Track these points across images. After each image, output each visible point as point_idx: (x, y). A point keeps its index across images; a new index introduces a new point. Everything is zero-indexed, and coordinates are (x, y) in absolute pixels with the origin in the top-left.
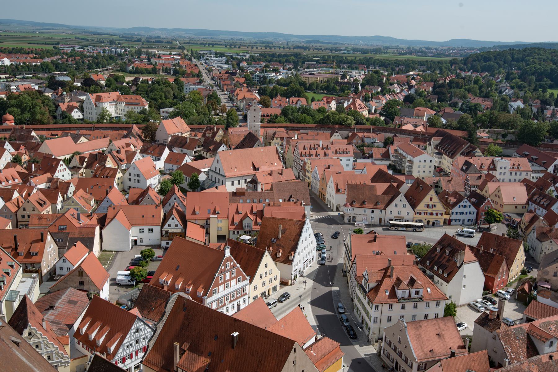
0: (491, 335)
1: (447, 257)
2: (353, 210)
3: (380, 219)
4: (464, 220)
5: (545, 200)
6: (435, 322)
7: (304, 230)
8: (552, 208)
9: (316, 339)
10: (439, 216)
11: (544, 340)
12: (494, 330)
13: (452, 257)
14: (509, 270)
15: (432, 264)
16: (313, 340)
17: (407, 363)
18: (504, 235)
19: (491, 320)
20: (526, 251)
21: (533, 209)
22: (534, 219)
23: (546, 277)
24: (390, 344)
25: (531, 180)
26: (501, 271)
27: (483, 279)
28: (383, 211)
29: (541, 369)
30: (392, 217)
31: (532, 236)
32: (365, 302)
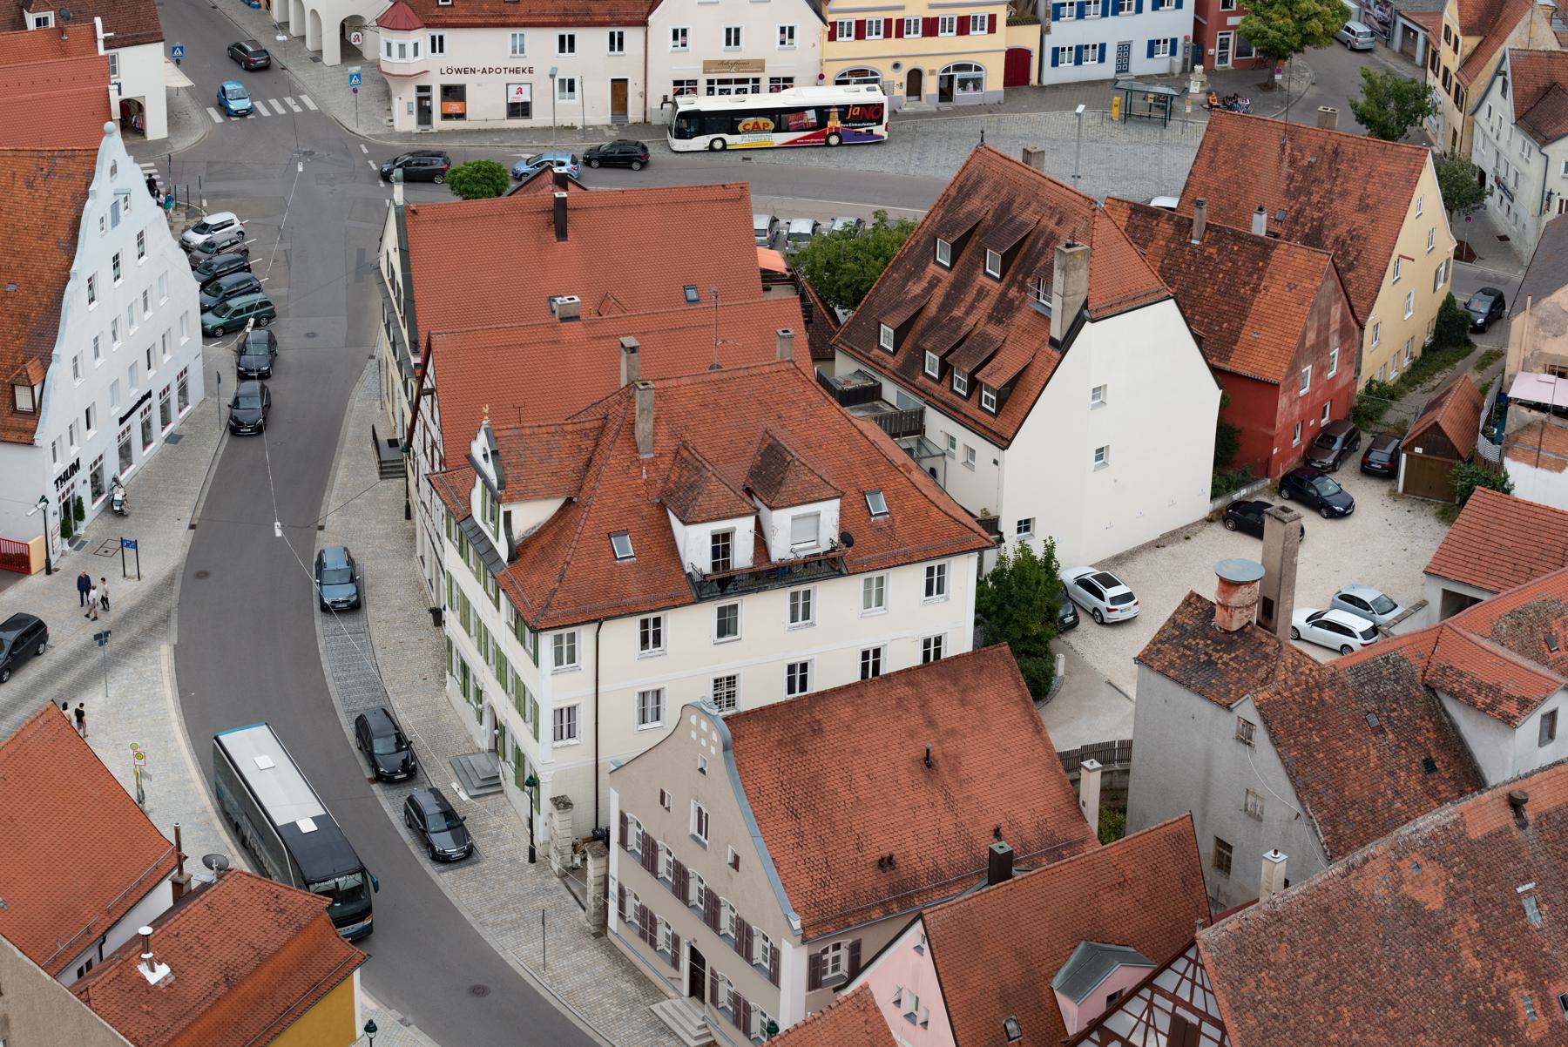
1: (996, 288)
2: (437, 45)
3: (619, 86)
4: (1124, 49)
6: (902, 690)
7: (94, 210)
9: (177, 886)
10: (977, 39)
11: (1511, 708)
13: (1022, 288)
15: (907, 345)
16: (163, 897)
17: (748, 957)
24: (649, 859)
27: (1212, 395)
28: (632, 36)
30: (689, 65)
32: (498, 621)
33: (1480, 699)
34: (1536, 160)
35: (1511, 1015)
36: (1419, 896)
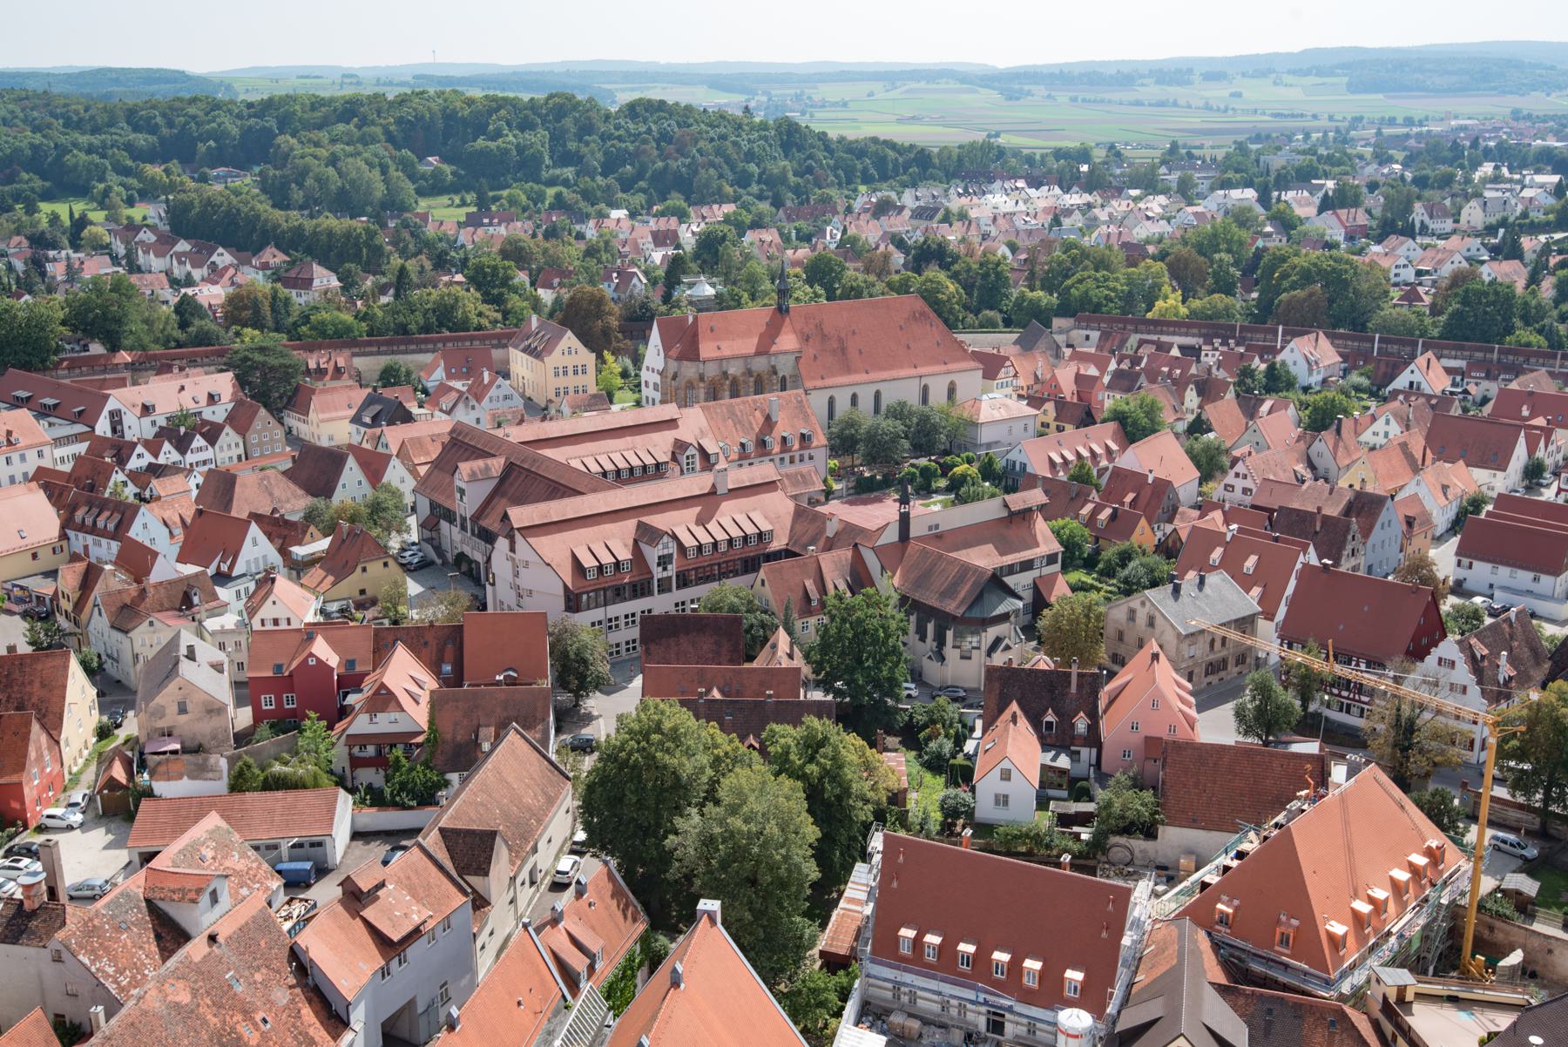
0: (46, 954)
5: (106, 514)
8: (132, 534)
11: (192, 895)
12: (49, 935)
14: (58, 743)
18: (12, 649)
19: (33, 914)
20: (91, 671)
21: (80, 551)
22: (90, 576)
23: (162, 724)
25: (60, 467)
26: (32, 754)
29: (196, 982)
31: (99, 624)
33: (175, 897)
34: (126, 642)
35: (239, 1038)
36: (177, 999)
